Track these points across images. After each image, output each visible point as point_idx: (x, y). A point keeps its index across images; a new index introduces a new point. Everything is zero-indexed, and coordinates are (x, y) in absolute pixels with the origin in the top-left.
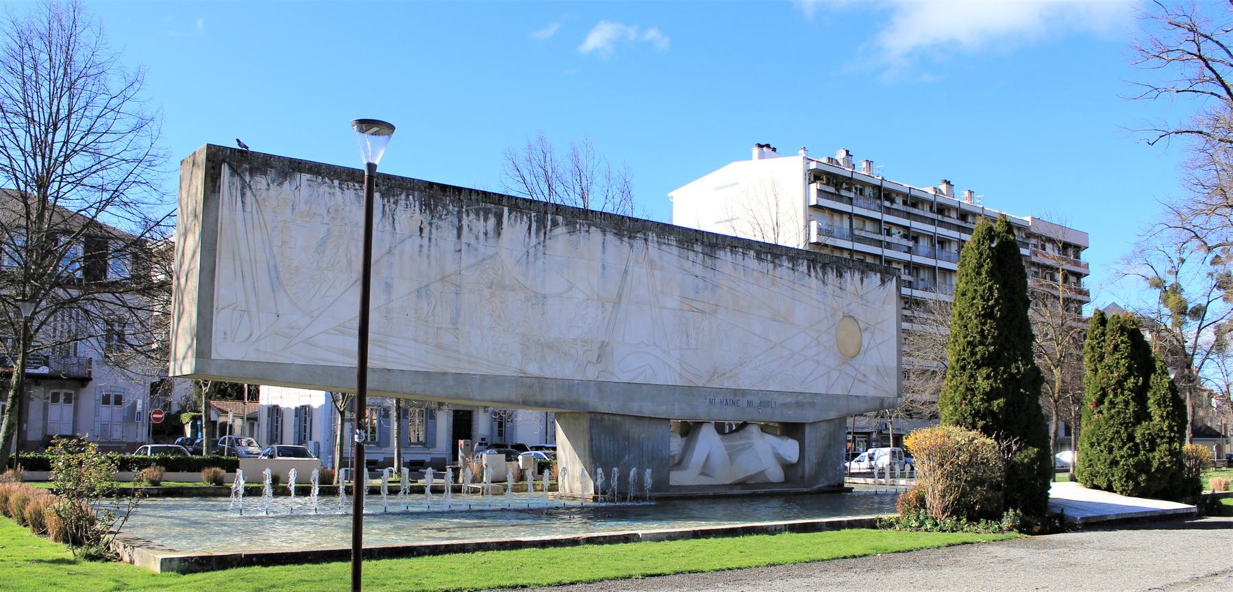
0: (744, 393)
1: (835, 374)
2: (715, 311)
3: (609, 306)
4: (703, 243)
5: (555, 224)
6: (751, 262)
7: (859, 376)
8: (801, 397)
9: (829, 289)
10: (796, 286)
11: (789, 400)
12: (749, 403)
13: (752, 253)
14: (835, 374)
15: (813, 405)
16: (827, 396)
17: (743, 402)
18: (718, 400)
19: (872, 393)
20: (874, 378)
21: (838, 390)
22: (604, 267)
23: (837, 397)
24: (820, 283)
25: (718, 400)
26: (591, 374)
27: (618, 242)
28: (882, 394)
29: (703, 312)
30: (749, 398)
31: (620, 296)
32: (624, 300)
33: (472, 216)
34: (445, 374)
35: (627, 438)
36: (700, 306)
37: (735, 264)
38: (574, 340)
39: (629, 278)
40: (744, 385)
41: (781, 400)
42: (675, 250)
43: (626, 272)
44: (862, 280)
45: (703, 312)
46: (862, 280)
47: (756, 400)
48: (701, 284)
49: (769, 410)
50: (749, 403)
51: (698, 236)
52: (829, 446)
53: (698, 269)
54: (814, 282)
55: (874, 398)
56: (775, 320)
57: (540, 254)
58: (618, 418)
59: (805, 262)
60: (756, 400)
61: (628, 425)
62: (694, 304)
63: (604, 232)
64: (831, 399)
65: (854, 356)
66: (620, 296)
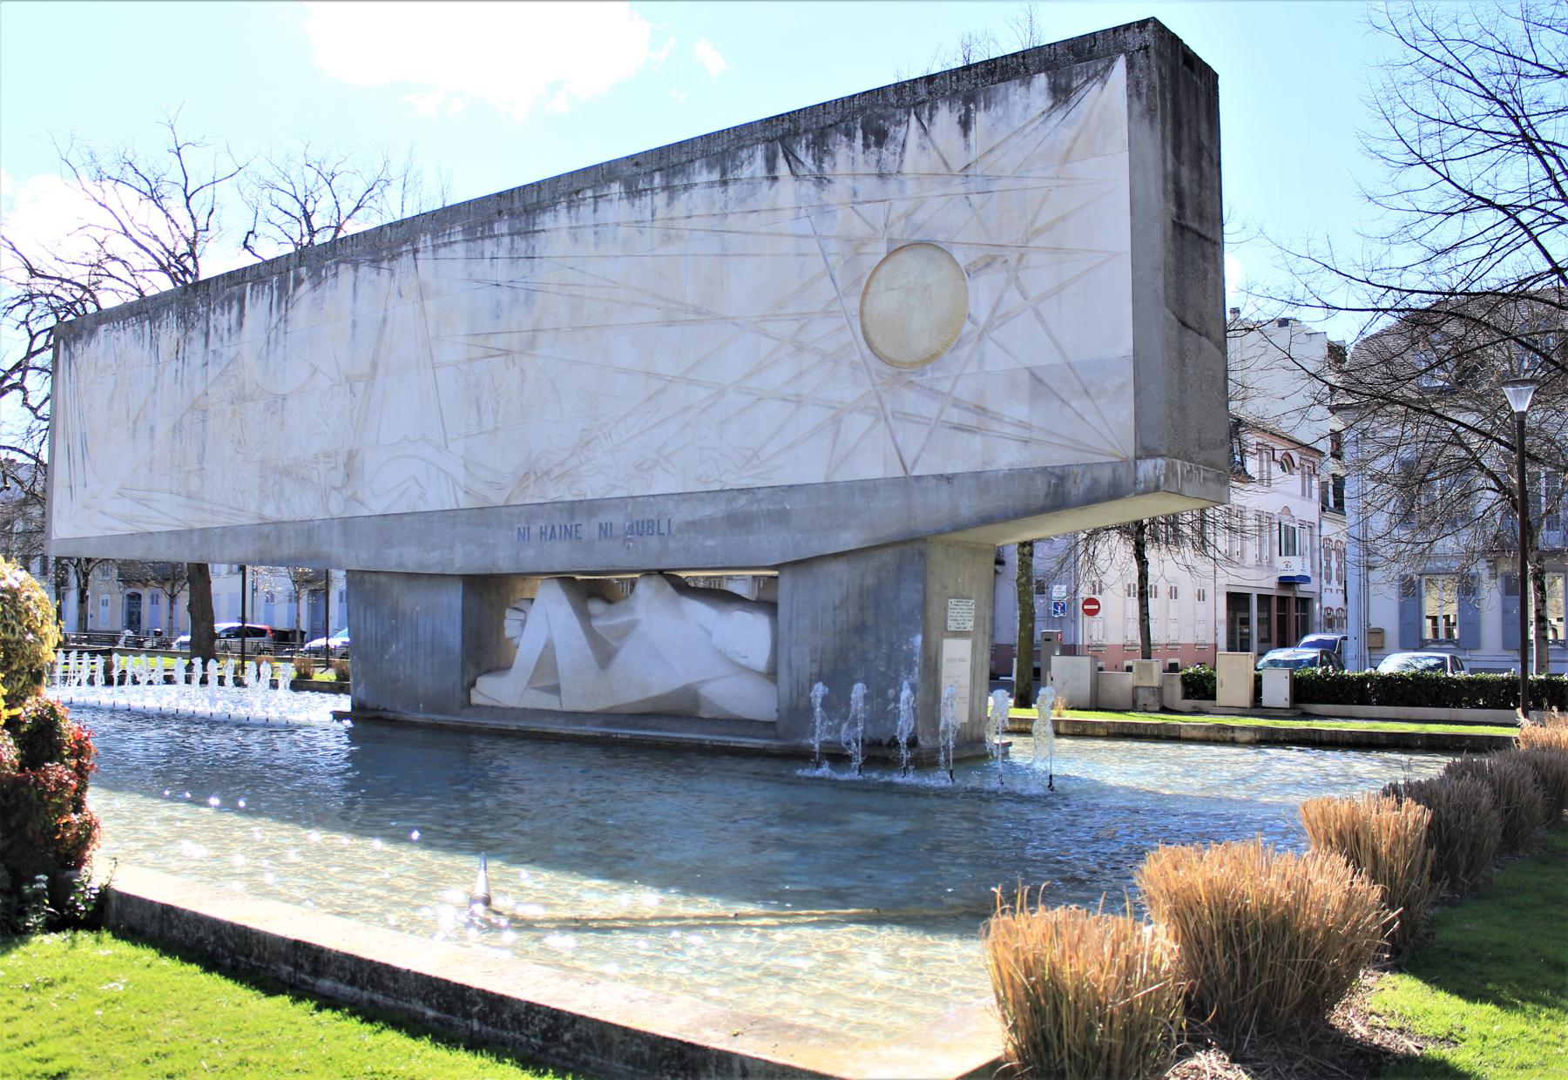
0: (591, 507)
1: (857, 425)
2: (532, 344)
3: (360, 387)
4: (512, 214)
5: (298, 282)
6: (616, 208)
7: (955, 416)
8: (742, 501)
9: (839, 190)
10: (734, 222)
11: (708, 511)
12: (605, 530)
13: (616, 188)
14: (857, 425)
15: (781, 518)
16: (830, 487)
17: (589, 529)
18: (535, 530)
19: (1008, 456)
20: (1019, 410)
21: (873, 467)
22: (354, 325)
23: (867, 488)
24: (808, 188)
25: (535, 530)
26: (336, 507)
27: (374, 275)
28: (1056, 457)
29: (508, 352)
30: (602, 518)
31: (374, 366)
32: (381, 371)
33: (218, 311)
34: (191, 531)
35: (394, 614)
36: (500, 342)
37: (575, 233)
38: (316, 456)
39: (388, 329)
40: (592, 487)
41: (683, 514)
42: (459, 250)
43: (384, 321)
44: (965, 124)
45: (508, 352)
46: (965, 124)
47: (619, 520)
48: (505, 296)
49: (654, 542)
50: (605, 530)
51: (504, 204)
52: (860, 629)
53: (502, 271)
54: (788, 190)
55: (1013, 475)
56: (670, 323)
57: (281, 336)
58: (383, 578)
59: (760, 153)
60: (619, 520)
61: (396, 589)
62: (494, 342)
63: (356, 266)
64: (837, 496)
65: (933, 357)
66: (374, 366)
